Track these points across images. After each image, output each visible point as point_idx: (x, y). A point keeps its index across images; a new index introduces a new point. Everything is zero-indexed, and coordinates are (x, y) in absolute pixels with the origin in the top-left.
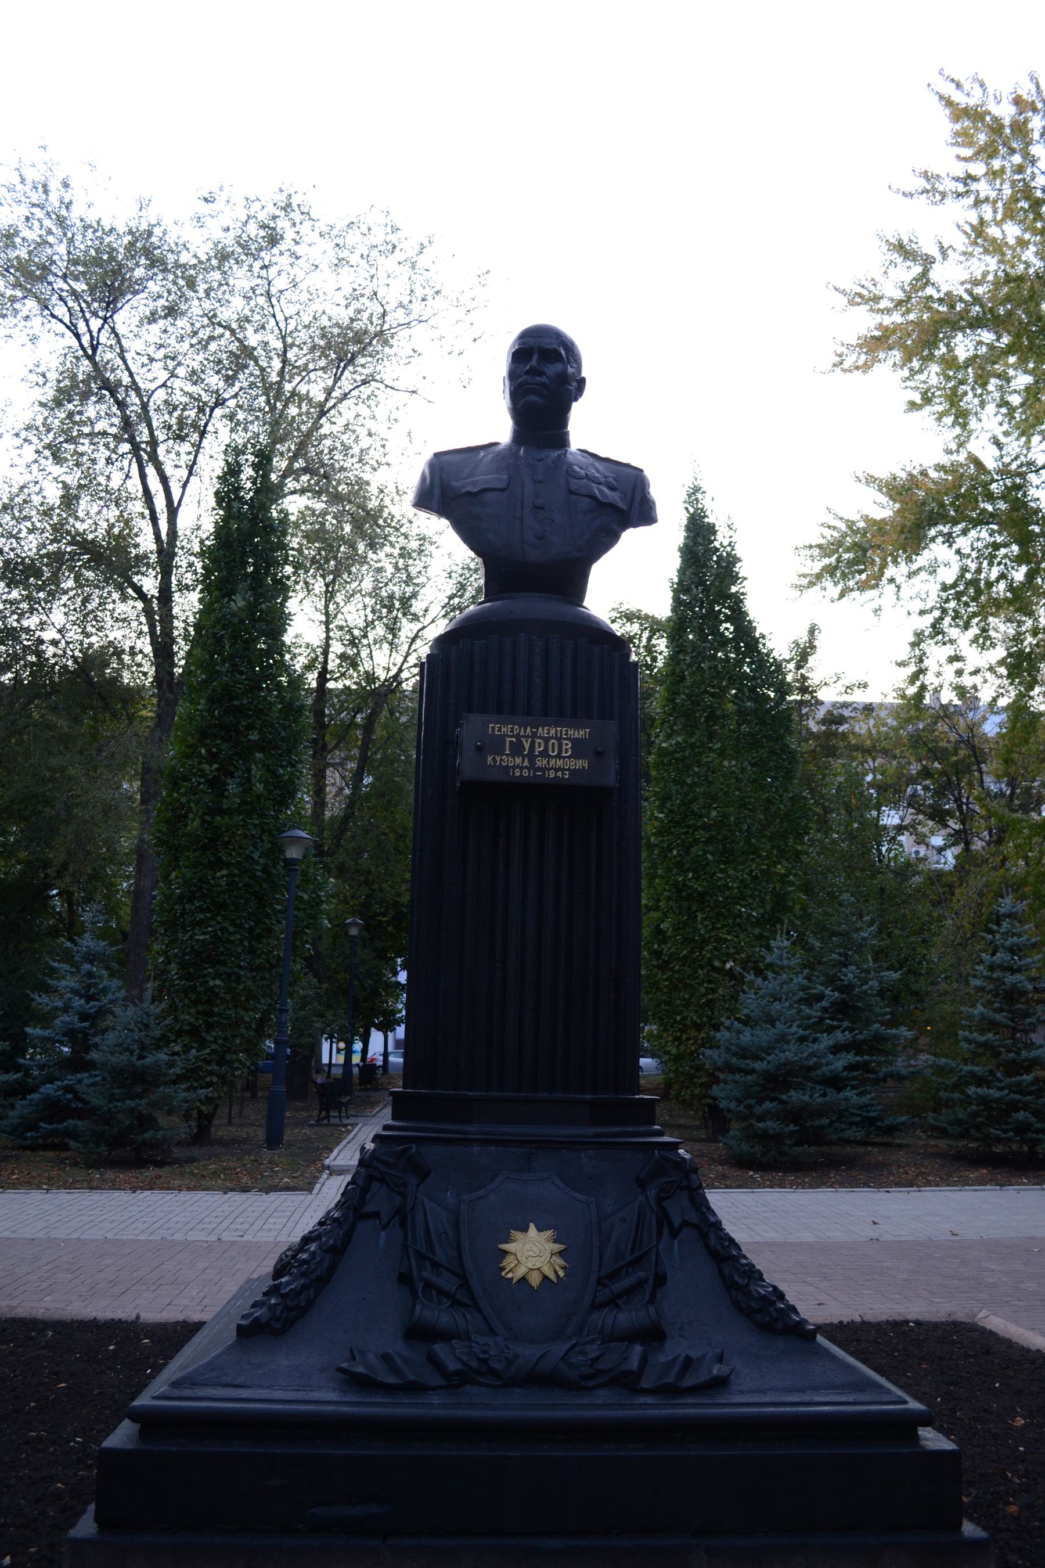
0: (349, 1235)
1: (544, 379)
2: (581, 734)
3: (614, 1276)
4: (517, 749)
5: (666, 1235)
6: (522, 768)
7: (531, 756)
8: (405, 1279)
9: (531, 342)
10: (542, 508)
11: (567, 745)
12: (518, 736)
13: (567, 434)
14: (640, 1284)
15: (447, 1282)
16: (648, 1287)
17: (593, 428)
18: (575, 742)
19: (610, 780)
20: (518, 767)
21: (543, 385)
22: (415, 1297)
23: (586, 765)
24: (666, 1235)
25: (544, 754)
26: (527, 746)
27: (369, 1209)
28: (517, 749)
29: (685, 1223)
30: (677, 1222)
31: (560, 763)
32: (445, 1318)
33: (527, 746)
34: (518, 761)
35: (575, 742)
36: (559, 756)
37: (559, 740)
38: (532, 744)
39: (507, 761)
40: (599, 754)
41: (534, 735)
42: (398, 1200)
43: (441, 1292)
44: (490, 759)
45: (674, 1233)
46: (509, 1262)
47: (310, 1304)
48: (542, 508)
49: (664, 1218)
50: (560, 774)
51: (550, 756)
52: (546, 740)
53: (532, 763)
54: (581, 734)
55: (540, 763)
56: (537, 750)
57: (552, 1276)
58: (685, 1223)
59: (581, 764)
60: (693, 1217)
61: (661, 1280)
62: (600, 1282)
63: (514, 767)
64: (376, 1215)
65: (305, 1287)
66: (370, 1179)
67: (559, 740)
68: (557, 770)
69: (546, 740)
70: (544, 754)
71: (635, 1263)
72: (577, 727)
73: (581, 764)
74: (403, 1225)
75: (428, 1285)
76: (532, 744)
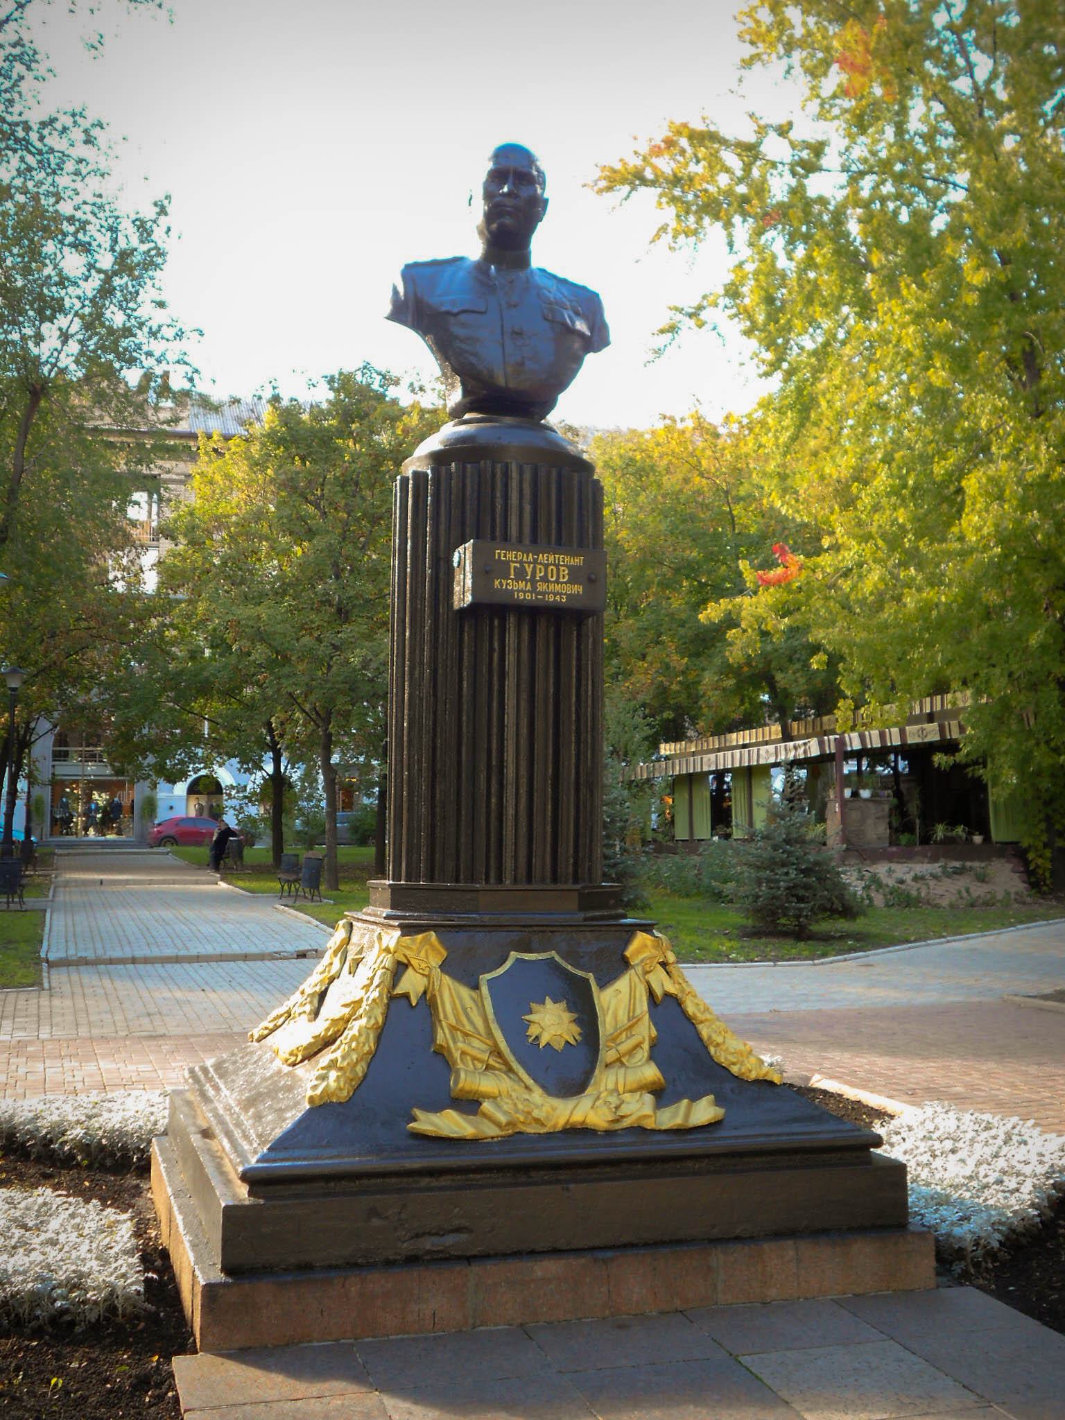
2: (577, 561)
4: (520, 575)
6: (525, 592)
7: (533, 581)
12: (521, 562)
13: (530, 253)
17: (551, 250)
23: (581, 591)
25: (544, 579)
26: (529, 571)
28: (520, 575)
31: (558, 588)
33: (529, 571)
34: (522, 585)
36: (557, 582)
37: (557, 566)
38: (534, 568)
39: (511, 585)
41: (535, 562)
44: (497, 582)
50: (558, 598)
51: (548, 581)
52: (546, 566)
54: (577, 561)
55: (541, 587)
56: (539, 575)
57: (573, 1042)
59: (577, 589)
63: (519, 591)
68: (555, 595)
69: (546, 566)
70: (544, 579)
72: (574, 555)
73: (577, 589)
76: (534, 568)
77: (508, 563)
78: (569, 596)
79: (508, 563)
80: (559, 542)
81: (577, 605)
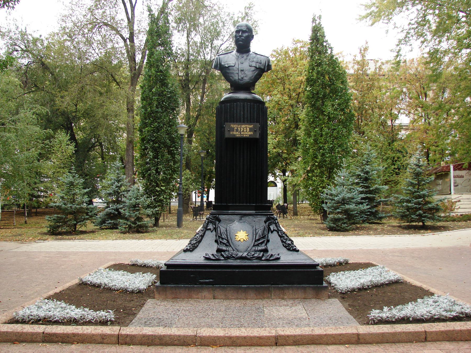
0: (204, 233)
1: (243, 38)
2: (251, 126)
3: (259, 240)
4: (237, 130)
5: (270, 232)
7: (240, 132)
8: (216, 241)
9: (240, 28)
10: (243, 71)
11: (248, 129)
14: (264, 241)
15: (225, 241)
16: (265, 242)
18: (250, 128)
19: (258, 136)
20: (237, 134)
21: (243, 39)
22: (218, 244)
24: (270, 232)
27: (208, 228)
28: (237, 130)
29: (274, 230)
30: (272, 230)
32: (224, 248)
34: (237, 133)
35: (250, 128)
39: (235, 133)
40: (255, 131)
42: (214, 226)
43: (224, 243)
45: (272, 232)
46: (237, 237)
47: (197, 246)
48: (243, 71)
49: (269, 229)
52: (244, 128)
53: (240, 133)
54: (251, 126)
56: (242, 130)
58: (274, 230)
59: (252, 133)
60: (276, 228)
61: (268, 241)
62: (255, 241)
64: (210, 229)
65: (196, 243)
66: (208, 222)
67: (246, 128)
70: (243, 131)
71: (263, 238)
72: (250, 125)
73: (252, 133)
74: (215, 231)
75: (221, 242)
77: (234, 128)
78: (250, 135)
79: (234, 128)
80: (244, 122)
81: (251, 137)
